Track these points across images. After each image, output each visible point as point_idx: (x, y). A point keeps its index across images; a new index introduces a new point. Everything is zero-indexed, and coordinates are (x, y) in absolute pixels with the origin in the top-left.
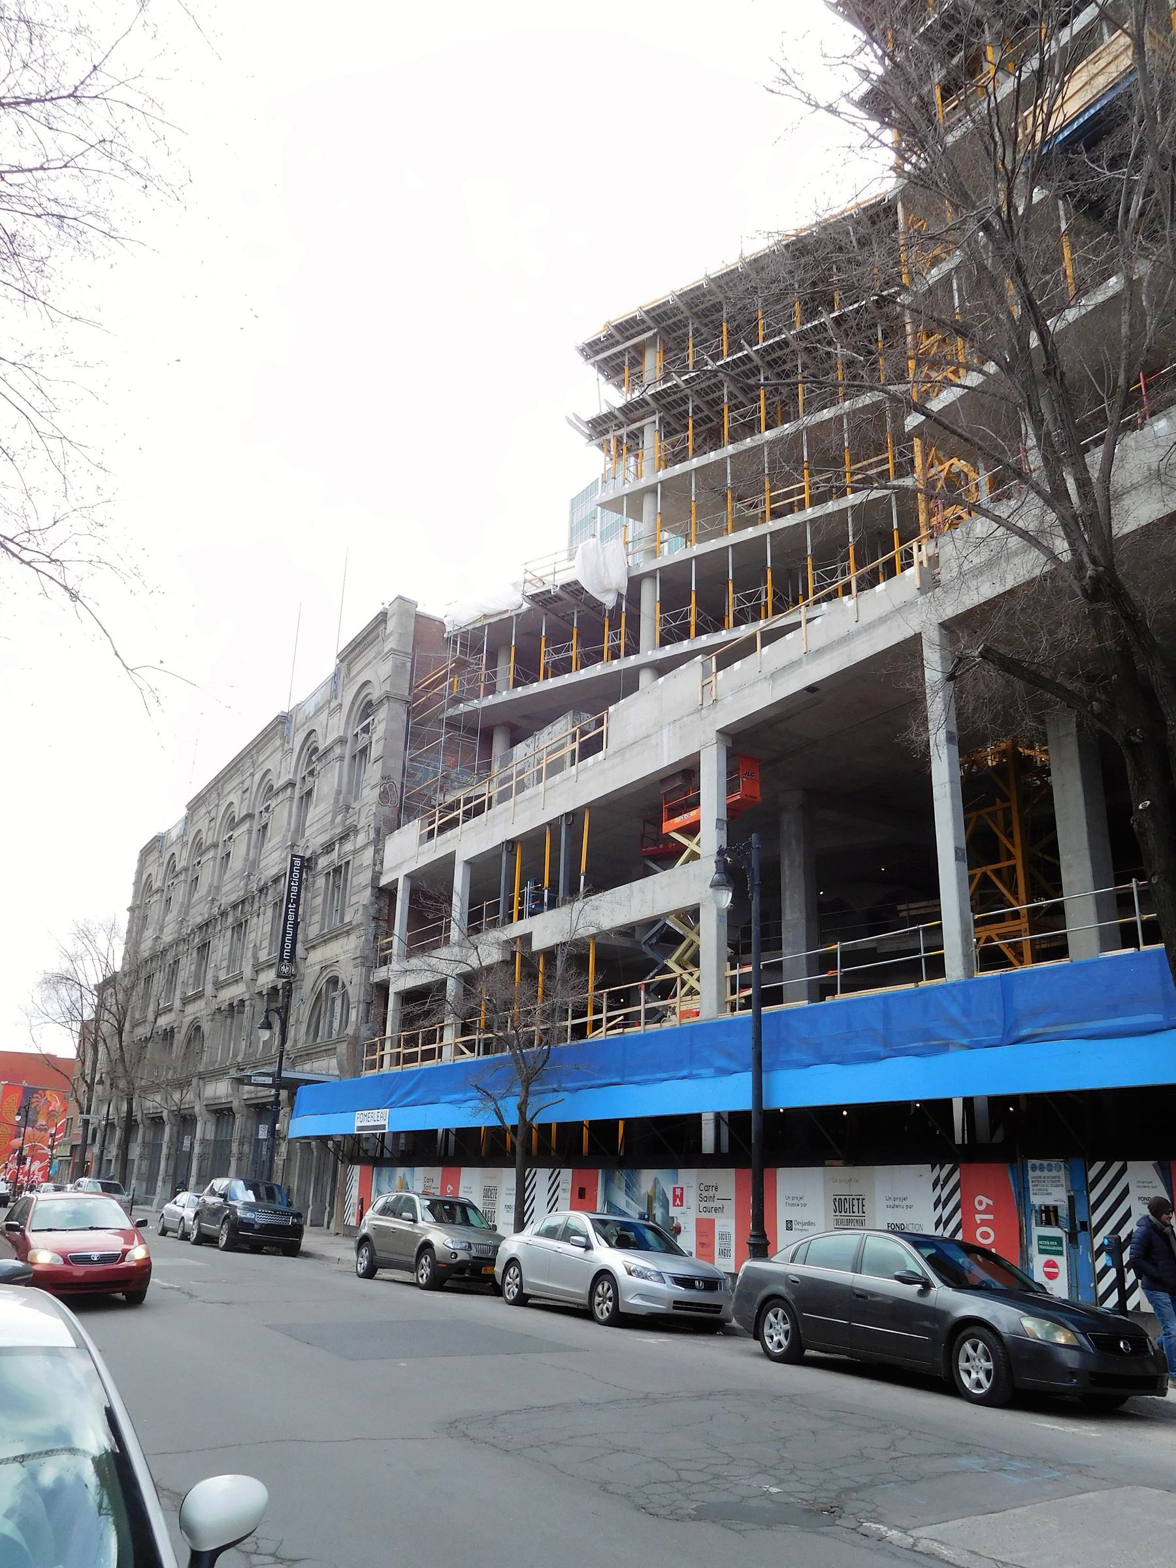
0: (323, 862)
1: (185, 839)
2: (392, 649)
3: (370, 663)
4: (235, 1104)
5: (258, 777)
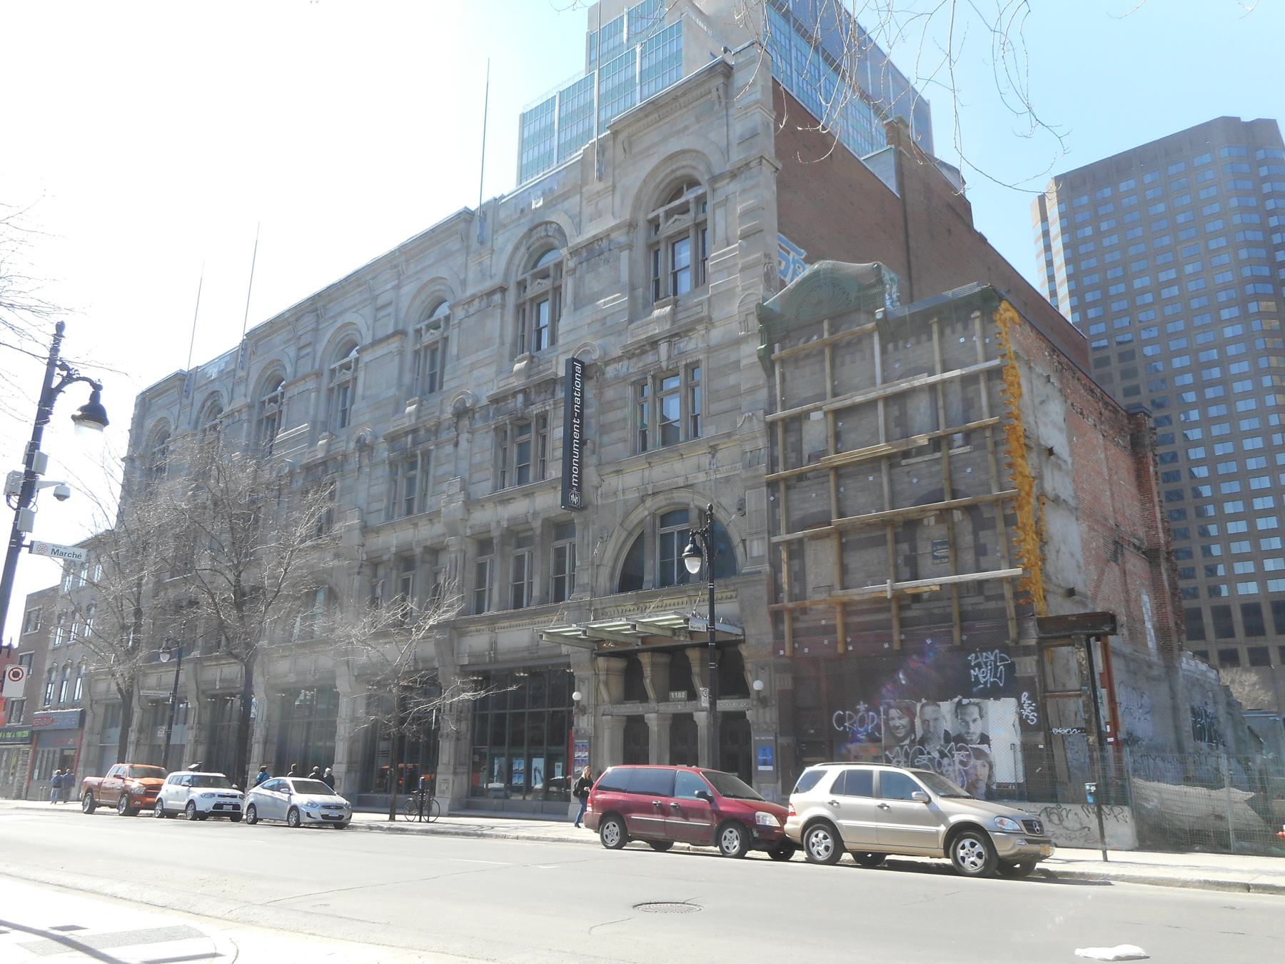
1: (241, 373)
2: (757, 102)
3: (686, 128)
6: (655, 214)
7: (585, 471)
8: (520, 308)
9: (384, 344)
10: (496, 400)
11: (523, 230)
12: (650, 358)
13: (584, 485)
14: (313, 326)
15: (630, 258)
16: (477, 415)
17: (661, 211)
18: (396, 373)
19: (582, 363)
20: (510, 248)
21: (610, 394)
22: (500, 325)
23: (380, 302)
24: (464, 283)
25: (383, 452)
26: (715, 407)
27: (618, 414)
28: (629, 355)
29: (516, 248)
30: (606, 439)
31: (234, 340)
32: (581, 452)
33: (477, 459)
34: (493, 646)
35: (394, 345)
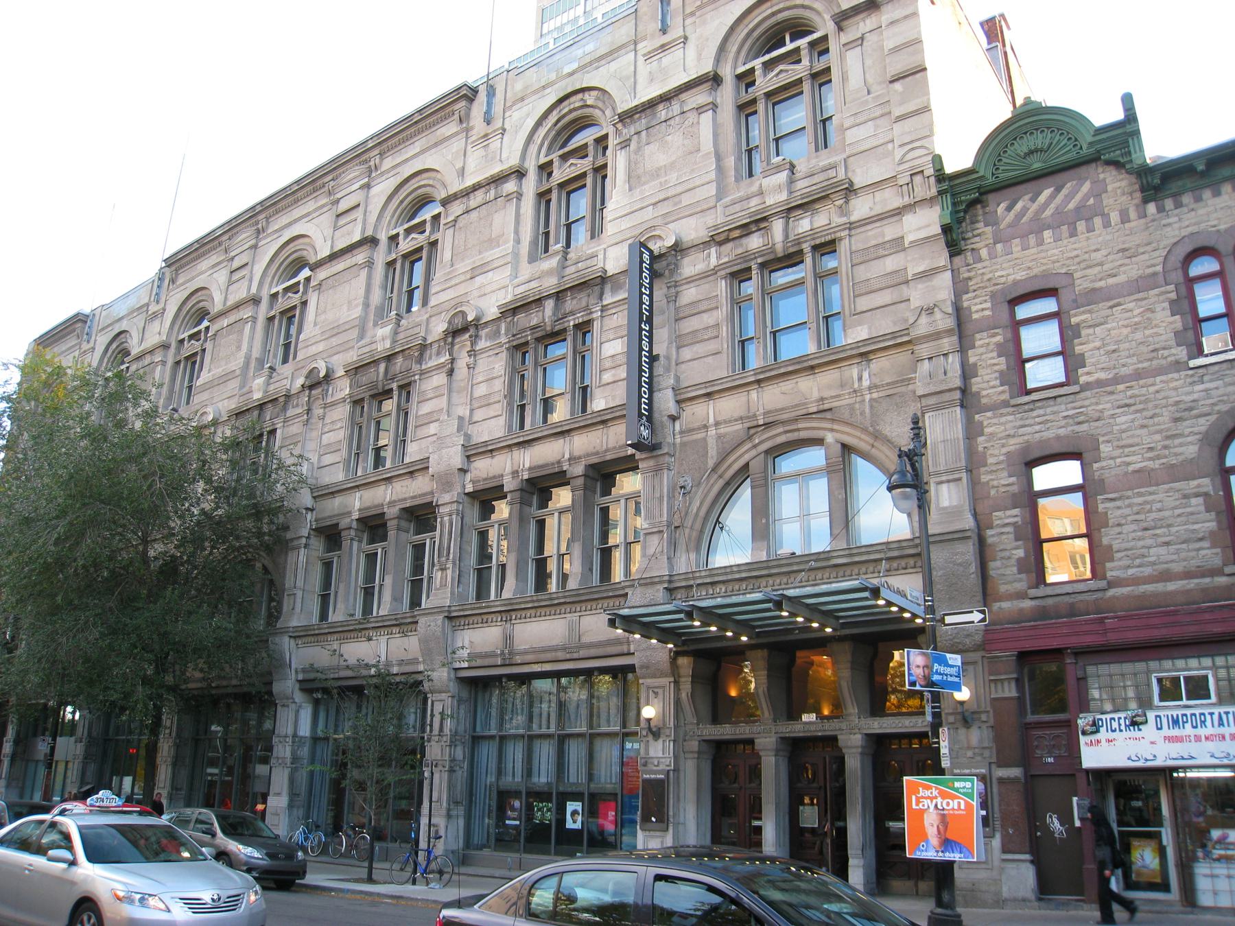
0: (690, 266)
1: (153, 308)
4: (441, 675)
5: (382, 188)
6: (748, 66)
7: (657, 396)
8: (543, 196)
9: (349, 255)
10: (512, 311)
11: (552, 99)
12: (755, 242)
13: (656, 415)
14: (253, 242)
15: (714, 120)
16: (483, 333)
17: (757, 63)
18: (362, 292)
19: (651, 251)
20: (531, 123)
21: (689, 294)
22: (513, 221)
23: (343, 206)
24: (462, 173)
25: (342, 389)
26: (863, 303)
27: (708, 319)
28: (718, 239)
29: (539, 124)
30: (687, 353)
31: (151, 267)
32: (651, 369)
33: (481, 390)
34: (508, 639)
35: (360, 257)
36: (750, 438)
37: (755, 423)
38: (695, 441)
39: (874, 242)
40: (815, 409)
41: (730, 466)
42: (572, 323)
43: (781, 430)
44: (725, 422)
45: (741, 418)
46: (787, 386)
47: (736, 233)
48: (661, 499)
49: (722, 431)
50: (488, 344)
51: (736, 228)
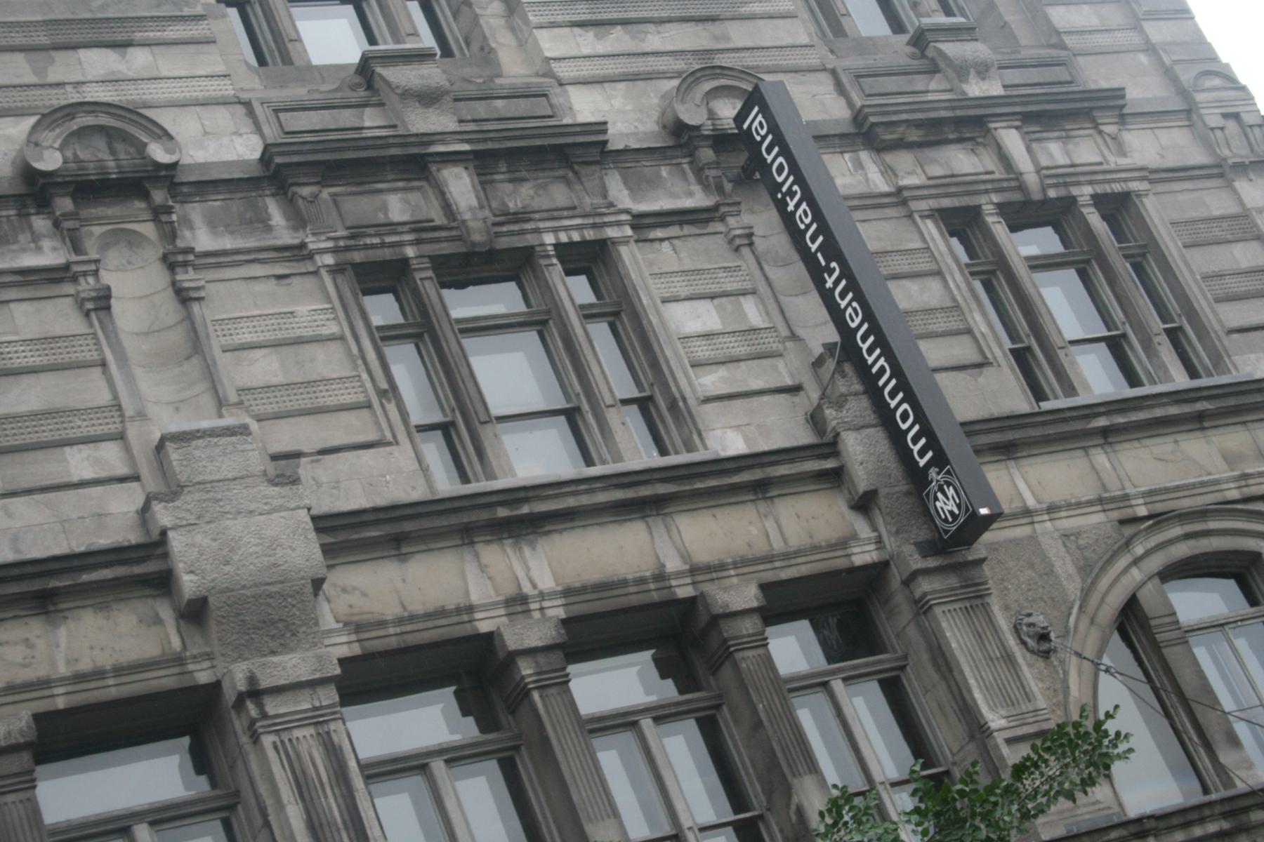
12: (963, 161)
36: (1128, 544)
37: (1127, 513)
38: (1015, 542)
39: (1194, 214)
40: (1235, 494)
41: (1102, 600)
42: (549, 239)
43: (1177, 531)
44: (1069, 506)
45: (1100, 501)
46: (1162, 446)
47: (914, 135)
48: (1009, 659)
49: (1067, 524)
50: (227, 243)
51: (918, 124)
